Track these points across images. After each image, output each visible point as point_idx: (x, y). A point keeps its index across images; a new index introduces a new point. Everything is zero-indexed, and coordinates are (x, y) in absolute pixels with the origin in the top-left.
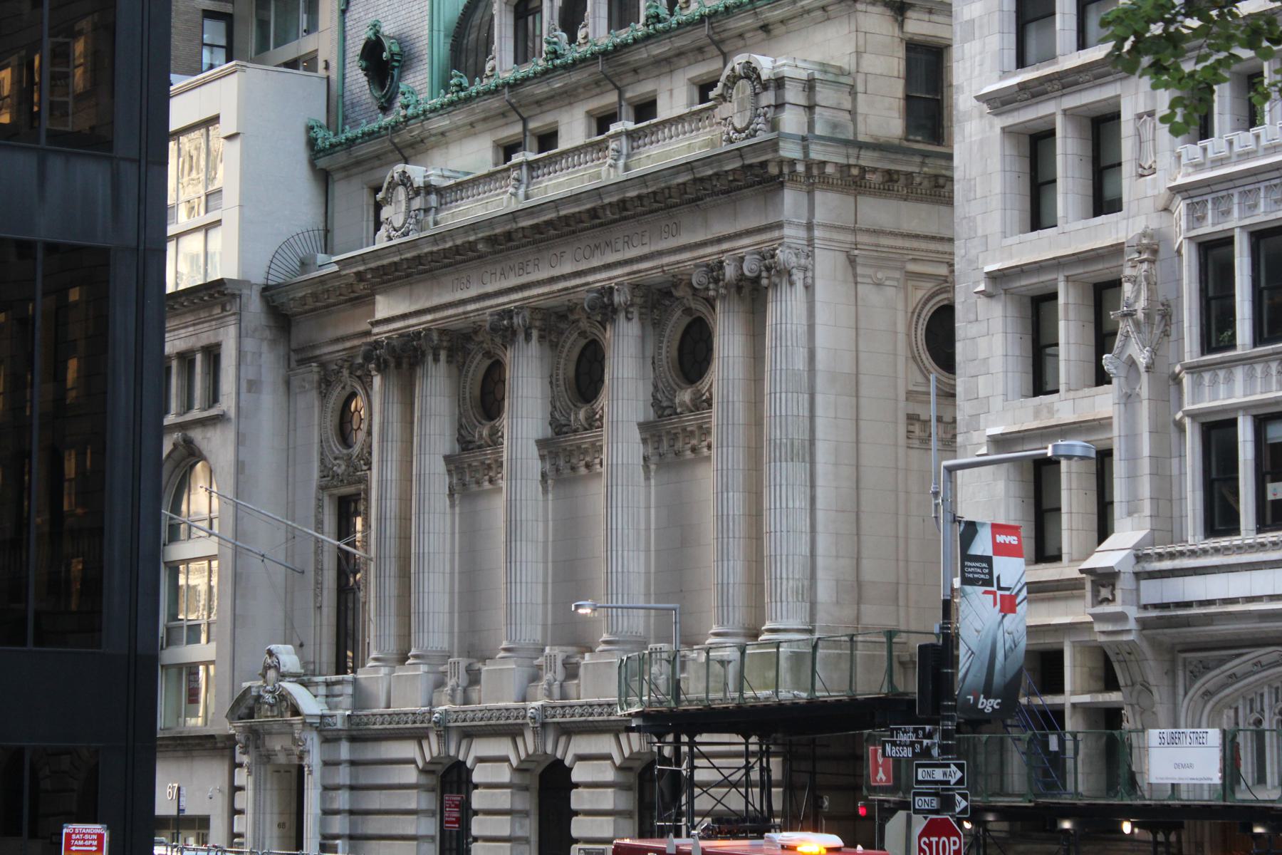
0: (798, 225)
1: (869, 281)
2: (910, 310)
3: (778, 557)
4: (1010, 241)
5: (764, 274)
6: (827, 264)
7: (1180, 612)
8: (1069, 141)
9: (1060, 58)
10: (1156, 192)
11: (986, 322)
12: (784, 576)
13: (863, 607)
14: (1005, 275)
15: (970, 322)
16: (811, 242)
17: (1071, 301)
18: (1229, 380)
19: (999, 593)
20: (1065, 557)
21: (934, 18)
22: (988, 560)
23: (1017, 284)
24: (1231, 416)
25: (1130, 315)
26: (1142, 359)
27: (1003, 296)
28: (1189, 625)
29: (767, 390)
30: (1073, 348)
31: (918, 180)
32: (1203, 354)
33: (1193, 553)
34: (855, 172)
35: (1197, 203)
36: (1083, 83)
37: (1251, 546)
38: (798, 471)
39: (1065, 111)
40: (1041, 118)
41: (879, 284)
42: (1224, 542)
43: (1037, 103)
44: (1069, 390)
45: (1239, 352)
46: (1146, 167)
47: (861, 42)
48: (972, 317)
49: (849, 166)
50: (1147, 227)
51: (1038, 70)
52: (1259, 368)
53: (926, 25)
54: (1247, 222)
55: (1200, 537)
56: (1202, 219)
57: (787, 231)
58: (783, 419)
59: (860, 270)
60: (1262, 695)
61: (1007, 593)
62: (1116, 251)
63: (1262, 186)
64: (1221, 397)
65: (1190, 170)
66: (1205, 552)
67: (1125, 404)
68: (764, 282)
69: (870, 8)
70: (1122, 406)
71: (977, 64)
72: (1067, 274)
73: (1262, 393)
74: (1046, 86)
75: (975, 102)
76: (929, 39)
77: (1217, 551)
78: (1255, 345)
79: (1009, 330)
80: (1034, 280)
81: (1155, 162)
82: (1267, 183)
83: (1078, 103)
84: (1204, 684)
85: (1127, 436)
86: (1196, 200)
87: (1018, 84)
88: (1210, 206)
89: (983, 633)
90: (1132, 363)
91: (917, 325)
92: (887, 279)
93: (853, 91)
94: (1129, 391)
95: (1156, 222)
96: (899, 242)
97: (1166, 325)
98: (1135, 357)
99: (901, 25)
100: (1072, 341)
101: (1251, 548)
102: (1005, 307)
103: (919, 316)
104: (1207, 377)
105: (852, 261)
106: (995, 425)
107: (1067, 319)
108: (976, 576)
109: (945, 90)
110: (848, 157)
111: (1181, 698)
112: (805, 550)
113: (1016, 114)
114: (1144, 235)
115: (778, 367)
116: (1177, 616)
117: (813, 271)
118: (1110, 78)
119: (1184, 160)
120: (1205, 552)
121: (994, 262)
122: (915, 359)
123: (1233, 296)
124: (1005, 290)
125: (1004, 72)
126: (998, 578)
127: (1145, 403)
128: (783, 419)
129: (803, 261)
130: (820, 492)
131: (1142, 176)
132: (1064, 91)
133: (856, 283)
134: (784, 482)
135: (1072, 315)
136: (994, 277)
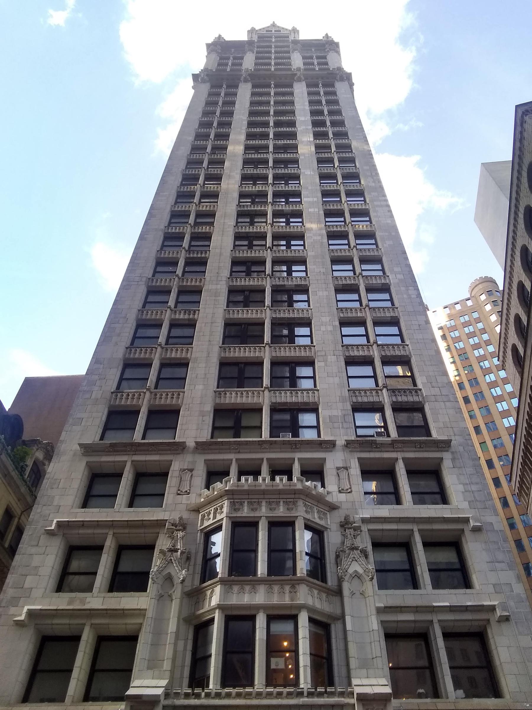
10: (189, 502)
11: (44, 548)
24: (252, 612)
35: (237, 502)
36: (150, 451)
39: (132, 461)
42: (248, 690)
43: (116, 455)
48: (35, 543)
62: (160, 524)
67: (158, 600)
70: (156, 602)
72: (115, 531)
80: (90, 531)
90: (169, 578)
95: (186, 515)
98: (173, 574)
104: (236, 588)
124: (64, 534)
131: (179, 494)
136: (60, 524)
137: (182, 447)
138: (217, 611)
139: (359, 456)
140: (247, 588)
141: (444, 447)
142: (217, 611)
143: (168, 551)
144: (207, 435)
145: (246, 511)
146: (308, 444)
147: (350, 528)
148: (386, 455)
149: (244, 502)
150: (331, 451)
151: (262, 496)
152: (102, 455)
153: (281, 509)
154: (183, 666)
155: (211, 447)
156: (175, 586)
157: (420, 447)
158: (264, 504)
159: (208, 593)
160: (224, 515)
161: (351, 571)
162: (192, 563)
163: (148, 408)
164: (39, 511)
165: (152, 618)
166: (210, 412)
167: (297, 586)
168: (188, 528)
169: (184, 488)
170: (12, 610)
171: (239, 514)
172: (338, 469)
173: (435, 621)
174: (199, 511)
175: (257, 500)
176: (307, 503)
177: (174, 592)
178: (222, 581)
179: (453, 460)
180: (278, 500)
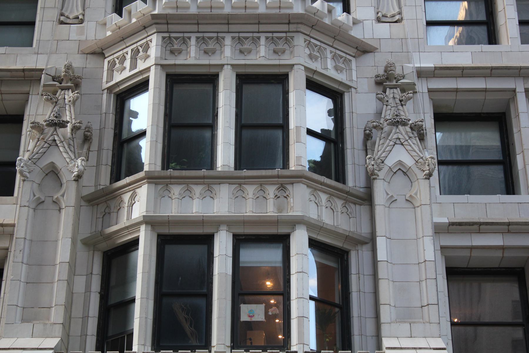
10: (83, 38)
24: (207, 230)
35: (177, 38)
46: (71, 17)
67: (34, 209)
70: (31, 211)
85: (31, 241)
95: (78, 62)
98: (59, 164)
131: (62, 23)
138: (143, 228)
140: (198, 189)
142: (143, 228)
143: (47, 125)
147: (395, 87)
149: (189, 38)
151: (225, 28)
153: (263, 50)
154: (85, 318)
156: (64, 186)
158: (228, 41)
159: (126, 197)
160: (151, 62)
161: (390, 161)
162: (95, 146)
165: (25, 238)
167: (289, 187)
168: (85, 87)
169: (71, 12)
171: (180, 60)
175: (215, 35)
176: (313, 41)
177: (63, 196)
178: (151, 178)
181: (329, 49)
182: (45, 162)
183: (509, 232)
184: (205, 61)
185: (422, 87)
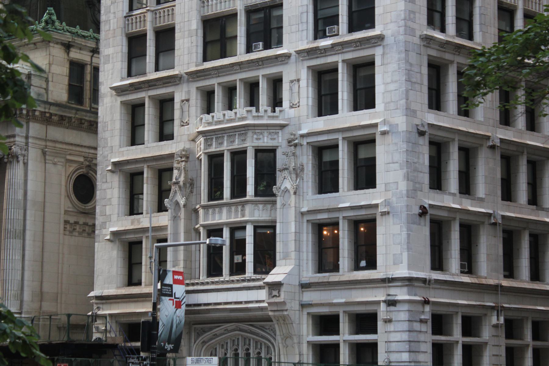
0: (22, 136)
1: (51, 162)
2: (67, 176)
3: (7, 281)
4: (122, 149)
5: (6, 157)
6: (33, 154)
7: (196, 308)
8: (151, 109)
9: (148, 74)
10: (189, 133)
12: (10, 289)
13: (43, 303)
14: (120, 164)
15: (103, 183)
16: (27, 144)
17: (149, 176)
18: (220, 212)
19: (175, 300)
20: (143, 284)
21: (82, 52)
22: (171, 286)
23: (126, 168)
24: (221, 227)
25: (177, 183)
26: (182, 202)
27: (119, 172)
28: (199, 314)
29: (4, 207)
30: (149, 196)
31: (73, 120)
32: (209, 201)
33: (202, 284)
34: (48, 115)
35: (209, 139)
36: (158, 85)
37: (228, 281)
38: (17, 243)
39: (149, 97)
40: (138, 98)
41: (55, 164)
42: (216, 279)
43: (137, 92)
44: (147, 213)
45: (224, 201)
46: (185, 122)
47: (51, 59)
48: (104, 180)
49: (45, 112)
50: (184, 147)
51: (138, 78)
52: (233, 208)
53: (78, 54)
54: (230, 148)
55: (205, 277)
56: (210, 145)
57: (17, 139)
58: (12, 220)
59: (47, 157)
60: (227, 343)
61: (178, 300)
62: (171, 156)
63: (237, 133)
64: (217, 219)
65: (206, 125)
66: (208, 283)
67: (173, 220)
68: (6, 160)
69: (56, 46)
70: (172, 221)
71: (110, 74)
72: (148, 164)
73: (234, 218)
74: (142, 85)
75: (109, 90)
76: (79, 60)
77: (213, 283)
78: (232, 198)
79: (121, 187)
80: (133, 166)
81: (189, 120)
82: (239, 133)
83: (155, 94)
84: (203, 338)
86: (208, 137)
87: (129, 84)
88: (214, 140)
89: (168, 317)
90: (177, 203)
91: (69, 183)
92: (59, 162)
93: (47, 80)
94: (175, 215)
95: (188, 145)
96: (64, 146)
97: (192, 188)
98: (178, 201)
99: (68, 54)
100: (149, 193)
101: (228, 282)
102: (119, 178)
103: (71, 178)
104: (211, 211)
105: (44, 153)
106: (113, 226)
107: (147, 183)
108: (166, 292)
109: (85, 83)
110: (45, 108)
111: (193, 344)
112: (19, 277)
113: (127, 96)
114: (183, 150)
115: (11, 198)
116: (195, 310)
117: (28, 156)
118: (170, 84)
119: (203, 121)
120: (208, 283)
121: (115, 157)
122: (68, 196)
123: (223, 178)
124: (120, 170)
125: (122, 78)
126: (175, 293)
127: (183, 221)
128: (12, 220)
129: (23, 152)
130: (27, 253)
132: (150, 88)
133: (45, 163)
134: (11, 248)
135: (149, 182)
136: (115, 164)
137: (178, 78)
139: (308, 65)
141: (376, 43)
144: (197, 58)
145: (214, 146)
146: (267, 60)
148: (330, 59)
150: (287, 63)
152: (128, 94)
154: (196, 261)
155: (198, 75)
157: (357, 46)
161: (282, 188)
162: (195, 186)
163: (154, 31)
164: (101, 153)
166: (197, 30)
167: (245, 206)
168: (190, 159)
170: (104, 231)
171: (210, 150)
172: (292, 82)
173: (341, 218)
174: (195, 141)
175: (221, 135)
179: (383, 55)
180: (235, 133)
181: (266, 131)
182: (174, 201)
183: (330, 211)
184: (218, 149)
185: (305, 142)
